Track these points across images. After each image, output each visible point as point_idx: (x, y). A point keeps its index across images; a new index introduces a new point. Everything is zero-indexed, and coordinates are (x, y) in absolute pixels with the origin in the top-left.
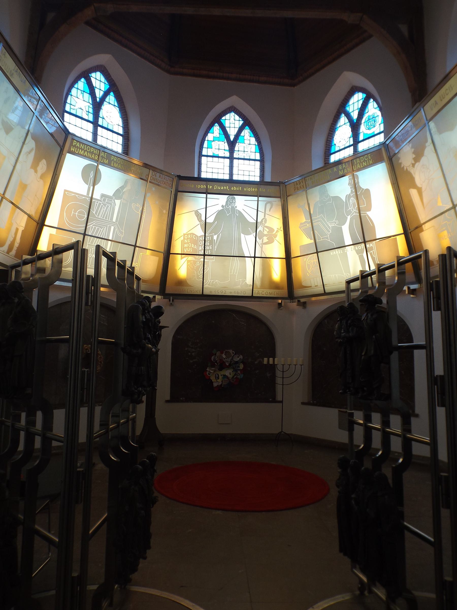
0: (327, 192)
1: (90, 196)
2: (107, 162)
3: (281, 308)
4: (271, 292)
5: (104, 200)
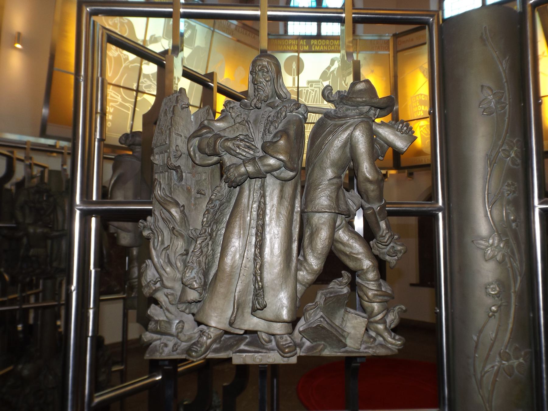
1: (296, 85)
2: (307, 48)
5: (311, 86)
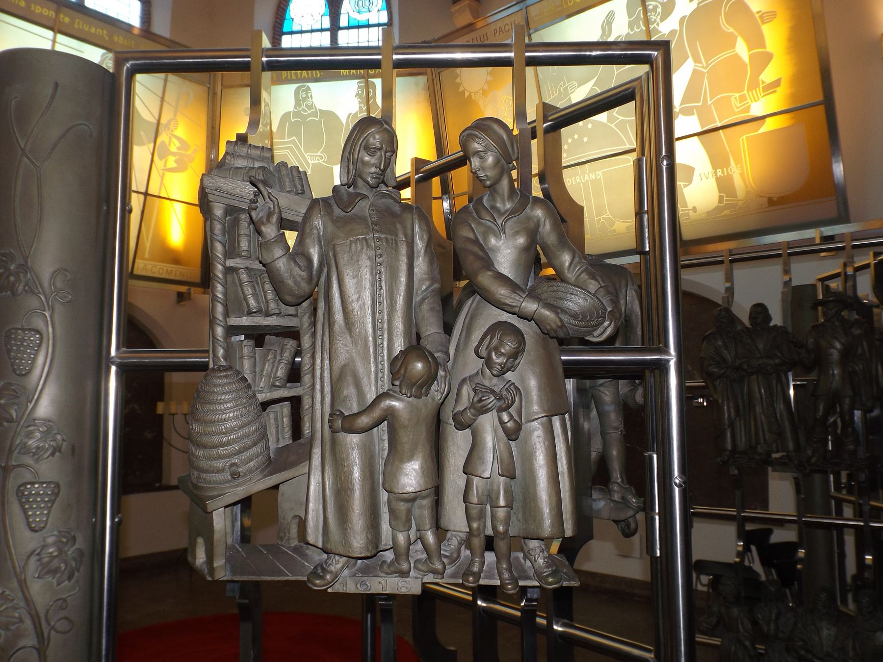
0: (312, 99)
3: (182, 303)
4: (170, 269)
